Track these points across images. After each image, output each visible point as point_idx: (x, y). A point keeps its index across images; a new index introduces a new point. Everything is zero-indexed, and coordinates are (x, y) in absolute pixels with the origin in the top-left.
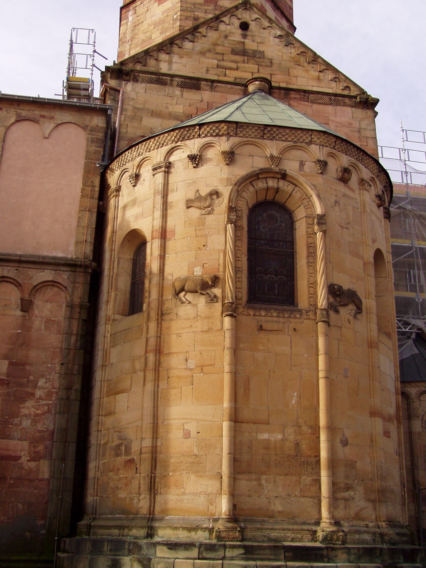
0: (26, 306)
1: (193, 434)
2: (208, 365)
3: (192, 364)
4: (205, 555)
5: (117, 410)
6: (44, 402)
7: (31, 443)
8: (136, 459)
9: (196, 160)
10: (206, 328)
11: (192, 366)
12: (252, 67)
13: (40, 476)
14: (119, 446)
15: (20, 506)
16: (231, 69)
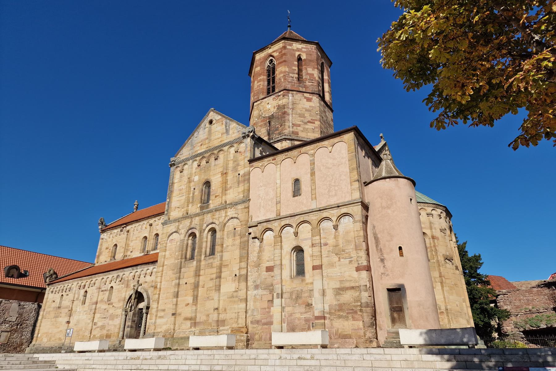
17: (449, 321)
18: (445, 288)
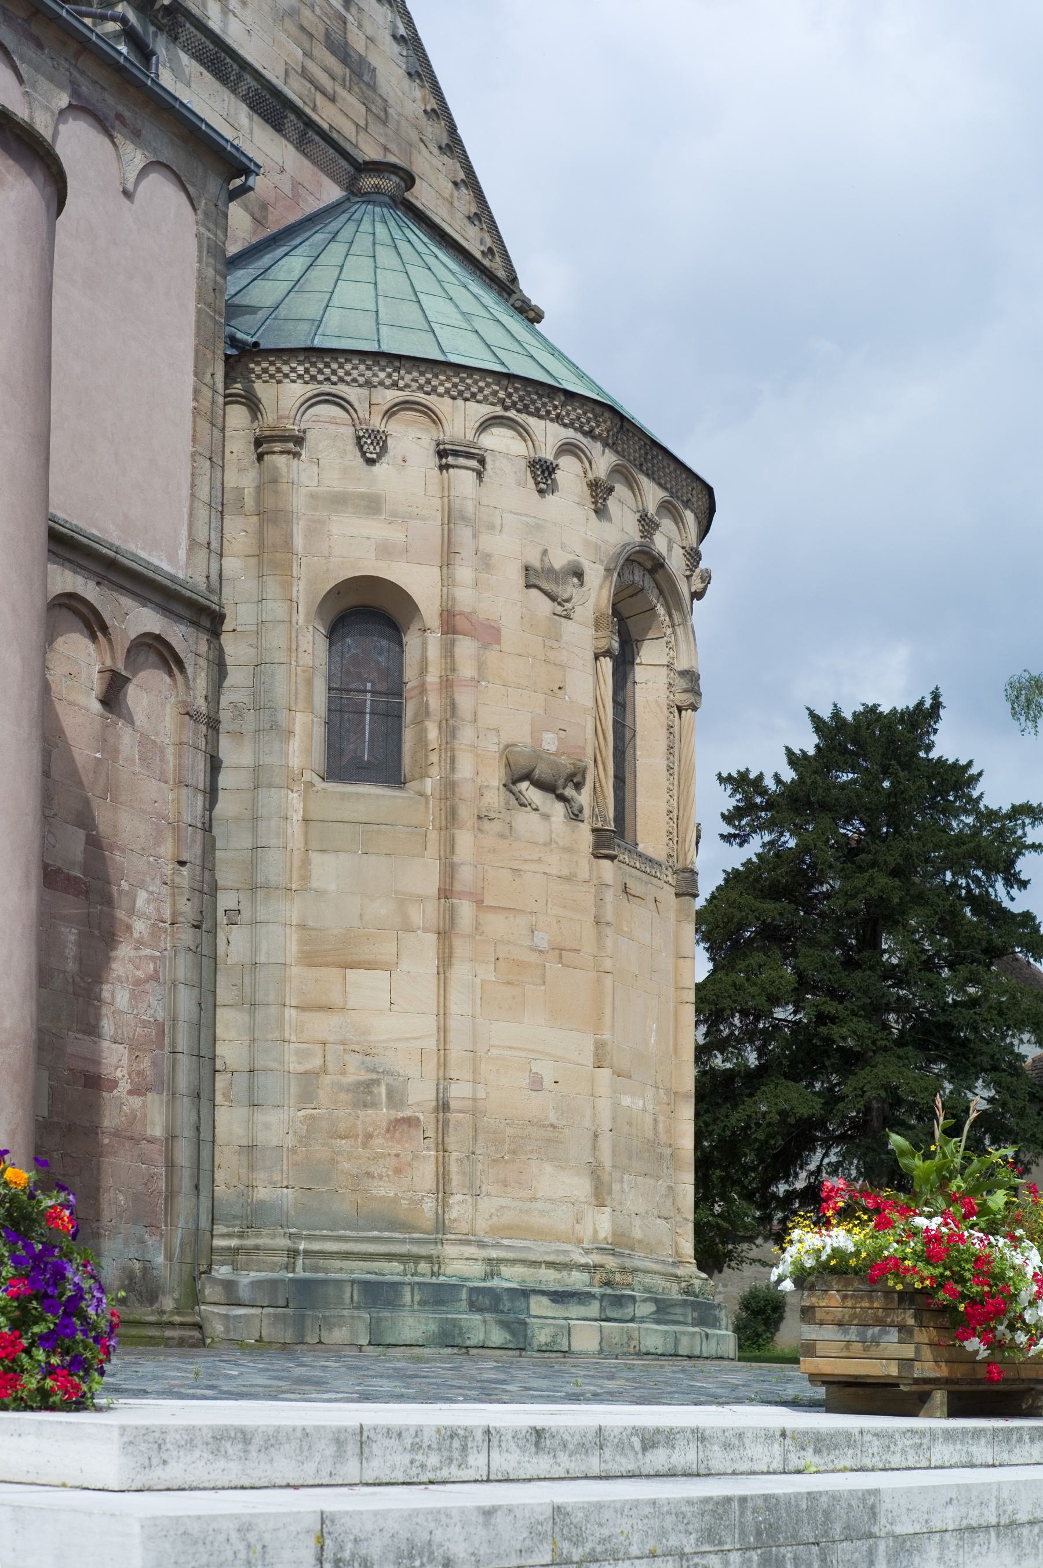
0: (113, 694)
1: (548, 1083)
2: (570, 950)
3: (542, 940)
4: (610, 1314)
5: (350, 1004)
6: (147, 952)
7: (132, 1048)
8: (422, 1118)
9: (543, 473)
10: (565, 872)
11: (544, 945)
12: (351, 101)
13: (149, 1132)
14: (368, 1086)
15: (121, 1197)
16: (324, 93)
17: (442, 1189)
18: (460, 971)
